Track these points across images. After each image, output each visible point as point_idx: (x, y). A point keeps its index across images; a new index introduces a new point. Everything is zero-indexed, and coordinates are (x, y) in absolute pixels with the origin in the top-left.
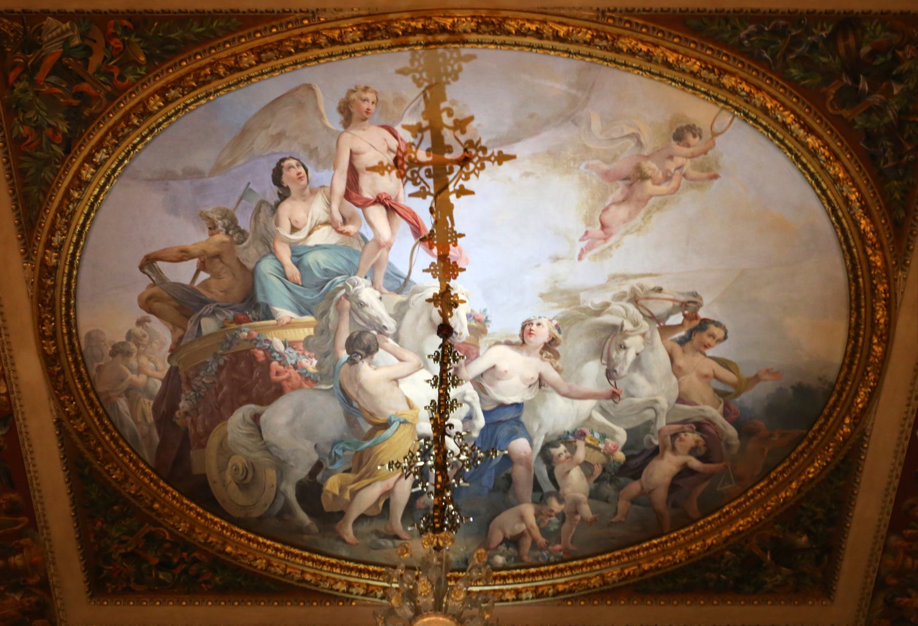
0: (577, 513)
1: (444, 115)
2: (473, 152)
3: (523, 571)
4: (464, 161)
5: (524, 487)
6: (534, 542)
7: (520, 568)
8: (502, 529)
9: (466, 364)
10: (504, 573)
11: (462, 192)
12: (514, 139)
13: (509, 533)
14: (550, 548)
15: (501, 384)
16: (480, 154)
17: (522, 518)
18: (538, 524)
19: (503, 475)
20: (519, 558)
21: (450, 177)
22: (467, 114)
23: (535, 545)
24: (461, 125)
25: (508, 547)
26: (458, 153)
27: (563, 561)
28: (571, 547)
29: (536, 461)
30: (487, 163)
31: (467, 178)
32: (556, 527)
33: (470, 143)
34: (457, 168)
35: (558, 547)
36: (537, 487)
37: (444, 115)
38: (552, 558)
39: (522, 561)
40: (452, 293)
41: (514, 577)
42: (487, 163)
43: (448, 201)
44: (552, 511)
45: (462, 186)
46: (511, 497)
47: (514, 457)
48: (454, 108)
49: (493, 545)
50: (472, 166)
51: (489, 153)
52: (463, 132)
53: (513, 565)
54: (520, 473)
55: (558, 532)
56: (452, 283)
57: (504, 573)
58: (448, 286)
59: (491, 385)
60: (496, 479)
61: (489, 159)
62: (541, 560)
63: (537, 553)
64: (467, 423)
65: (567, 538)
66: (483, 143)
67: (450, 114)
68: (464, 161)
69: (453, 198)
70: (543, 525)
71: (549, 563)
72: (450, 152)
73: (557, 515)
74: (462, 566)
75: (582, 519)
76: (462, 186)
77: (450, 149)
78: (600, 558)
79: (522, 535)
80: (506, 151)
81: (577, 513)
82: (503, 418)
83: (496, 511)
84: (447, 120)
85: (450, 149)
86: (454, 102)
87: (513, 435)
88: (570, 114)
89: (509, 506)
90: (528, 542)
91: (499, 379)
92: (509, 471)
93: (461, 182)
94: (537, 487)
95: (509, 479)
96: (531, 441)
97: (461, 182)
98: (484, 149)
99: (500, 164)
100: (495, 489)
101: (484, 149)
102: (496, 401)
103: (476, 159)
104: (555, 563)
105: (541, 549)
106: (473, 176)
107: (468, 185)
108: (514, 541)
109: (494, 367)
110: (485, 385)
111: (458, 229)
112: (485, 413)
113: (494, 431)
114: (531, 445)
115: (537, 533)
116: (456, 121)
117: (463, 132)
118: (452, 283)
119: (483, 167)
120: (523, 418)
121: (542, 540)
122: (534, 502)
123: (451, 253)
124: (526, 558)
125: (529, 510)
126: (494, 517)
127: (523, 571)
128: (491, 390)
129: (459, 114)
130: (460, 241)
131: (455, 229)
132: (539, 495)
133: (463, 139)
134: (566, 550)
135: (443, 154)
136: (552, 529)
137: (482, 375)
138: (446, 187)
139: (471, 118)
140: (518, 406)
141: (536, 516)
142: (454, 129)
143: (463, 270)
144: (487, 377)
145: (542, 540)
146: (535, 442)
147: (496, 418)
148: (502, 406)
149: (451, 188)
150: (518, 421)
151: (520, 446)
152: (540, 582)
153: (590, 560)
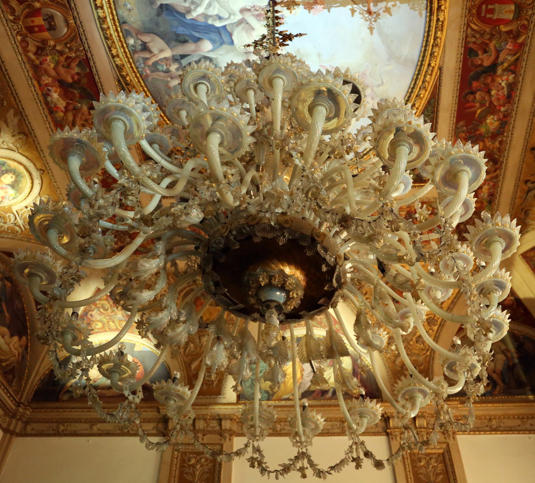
0: (172, 78)
1: (393, 3)
2: (374, 16)
4: (369, 12)
5: (181, 50)
6: (148, 59)
7: (130, 54)
8: (152, 40)
9: (253, 15)
11: (353, 11)
12: (381, 34)
13: (150, 45)
14: (147, 68)
15: (244, 34)
16: (373, 19)
17: (161, 51)
18: (160, 60)
19: (187, 38)
20: (135, 52)
21: (361, 6)
22: (393, 13)
23: (145, 60)
24: (387, 10)
25: (141, 45)
26: (373, 9)
27: (141, 76)
28: (150, 79)
29: (199, 55)
30: (368, 23)
31: (360, 13)
32: (161, 69)
33: (378, 15)
34: (366, 9)
36: (183, 57)
37: (393, 3)
38: (140, 69)
39: (134, 54)
40: (295, 7)
41: (125, 52)
42: (368, 23)
43: (348, 5)
44: (170, 66)
45: (356, 11)
46: (174, 43)
47: (199, 43)
48: (396, 8)
49: (140, 37)
50: (367, 15)
51: (374, 23)
52: (384, 11)
54: (189, 47)
55: (158, 70)
56: (301, 7)
57: (125, 45)
58: (299, 5)
59: (243, 28)
60: (183, 35)
61: (371, 23)
62: (138, 64)
63: (141, 61)
64: (216, 17)
65: (155, 75)
66: (378, 20)
67: (393, 6)
68: (369, 12)
69: (350, 7)
70: (160, 62)
71: (137, 68)
72: (374, 6)
73: (168, 69)
74: (121, 21)
76: (356, 11)
77: (376, 5)
79: (150, 52)
80: (375, 31)
81: (172, 78)
82: (223, 36)
83: (163, 36)
84: (390, 4)
85: (376, 5)
86: (399, 7)
87: (213, 41)
88: (392, 56)
89: (168, 43)
90: (147, 55)
91: (247, 32)
92: (190, 41)
93: (358, 11)
94: (183, 57)
95: (185, 42)
96: (212, 51)
97: (358, 11)
98: (375, 21)
99: (368, 28)
100: (178, 35)
101: (375, 21)
102: (233, 30)
103: (370, 17)
104: (138, 72)
105: (144, 63)
106: (362, 16)
107: (357, 14)
108: (145, 48)
109: (253, 29)
110: (242, 25)
111: (333, 10)
112: (224, 27)
113: (213, 32)
114: (209, 51)
115: (154, 60)
116: (390, 8)
117: (384, 11)
118: (301, 7)
119: (366, 20)
120: (224, 46)
121: (150, 63)
122: (173, 56)
123: (319, 6)
124: (136, 56)
125: (168, 53)
126: (158, 36)
127: (129, 56)
128: (240, 28)
129: (393, 10)
130: (326, 10)
131: (333, 8)
132: (179, 58)
133: (381, 12)
134: (147, 76)
135: (373, 2)
136: (158, 67)
137: (248, 23)
138: (355, 4)
139: (391, 15)
140: (232, 43)
141: (165, 58)
142: (386, 8)
143: (309, 12)
144: (247, 26)
145: (150, 63)
146: (211, 53)
147: (222, 32)
148: (231, 35)
149: (355, 6)
150: (222, 43)
151: (206, 46)
152: (127, 66)
153: (145, 89)
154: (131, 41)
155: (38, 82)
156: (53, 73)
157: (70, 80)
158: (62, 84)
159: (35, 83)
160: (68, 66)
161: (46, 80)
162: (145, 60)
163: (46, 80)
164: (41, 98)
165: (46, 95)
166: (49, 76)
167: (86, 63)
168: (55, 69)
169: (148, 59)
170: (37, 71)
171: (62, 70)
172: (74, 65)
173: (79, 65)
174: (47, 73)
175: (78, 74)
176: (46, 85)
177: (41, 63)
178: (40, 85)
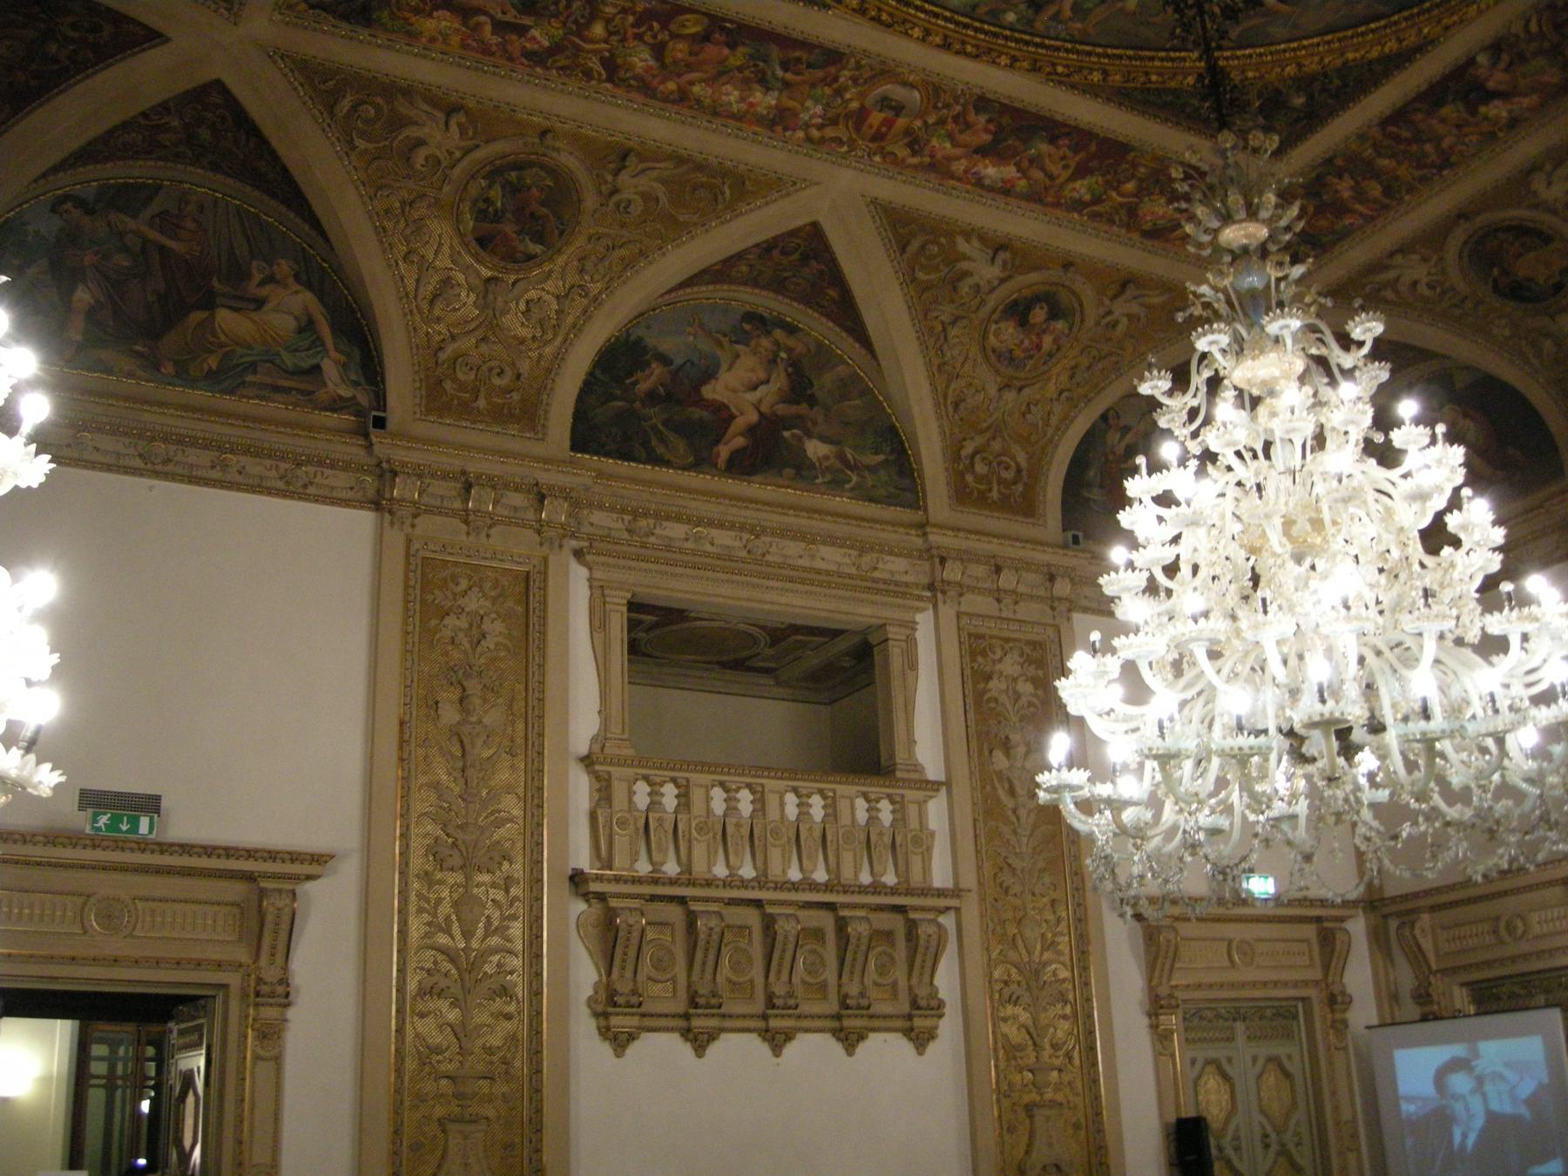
3: (1027, 37)
6: (1058, 13)
10: (1008, 33)
20: (1030, 23)
23: (1056, 17)
35: (1079, 25)
38: (1063, 34)
53: (1019, 27)
75: (1122, 9)
78: (1109, 51)
124: (1039, 25)
127: (1027, 37)
154: (1011, 17)
155: (952, 177)
156: (958, 151)
157: (989, 137)
158: (982, 151)
159: (952, 182)
160: (968, 125)
161: (959, 167)
162: (1056, 17)
163: (959, 167)
164: (979, 191)
165: (979, 182)
166: (958, 158)
167: (982, 103)
168: (955, 144)
169: (1058, 13)
170: (938, 169)
171: (965, 137)
172: (972, 117)
173: (978, 110)
174: (949, 159)
175: (989, 121)
176: (966, 171)
177: (932, 156)
178: (959, 180)
